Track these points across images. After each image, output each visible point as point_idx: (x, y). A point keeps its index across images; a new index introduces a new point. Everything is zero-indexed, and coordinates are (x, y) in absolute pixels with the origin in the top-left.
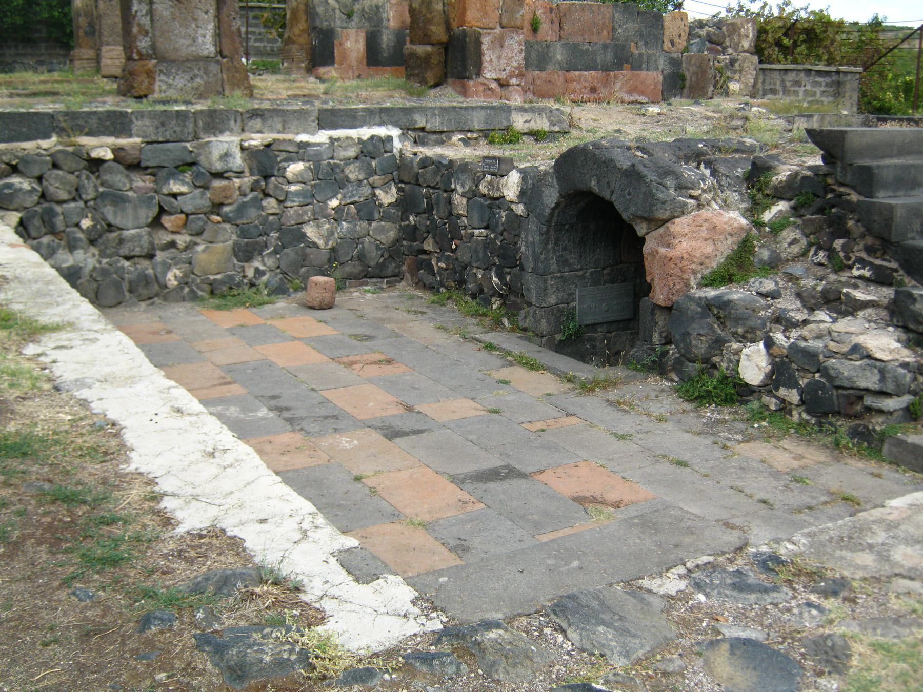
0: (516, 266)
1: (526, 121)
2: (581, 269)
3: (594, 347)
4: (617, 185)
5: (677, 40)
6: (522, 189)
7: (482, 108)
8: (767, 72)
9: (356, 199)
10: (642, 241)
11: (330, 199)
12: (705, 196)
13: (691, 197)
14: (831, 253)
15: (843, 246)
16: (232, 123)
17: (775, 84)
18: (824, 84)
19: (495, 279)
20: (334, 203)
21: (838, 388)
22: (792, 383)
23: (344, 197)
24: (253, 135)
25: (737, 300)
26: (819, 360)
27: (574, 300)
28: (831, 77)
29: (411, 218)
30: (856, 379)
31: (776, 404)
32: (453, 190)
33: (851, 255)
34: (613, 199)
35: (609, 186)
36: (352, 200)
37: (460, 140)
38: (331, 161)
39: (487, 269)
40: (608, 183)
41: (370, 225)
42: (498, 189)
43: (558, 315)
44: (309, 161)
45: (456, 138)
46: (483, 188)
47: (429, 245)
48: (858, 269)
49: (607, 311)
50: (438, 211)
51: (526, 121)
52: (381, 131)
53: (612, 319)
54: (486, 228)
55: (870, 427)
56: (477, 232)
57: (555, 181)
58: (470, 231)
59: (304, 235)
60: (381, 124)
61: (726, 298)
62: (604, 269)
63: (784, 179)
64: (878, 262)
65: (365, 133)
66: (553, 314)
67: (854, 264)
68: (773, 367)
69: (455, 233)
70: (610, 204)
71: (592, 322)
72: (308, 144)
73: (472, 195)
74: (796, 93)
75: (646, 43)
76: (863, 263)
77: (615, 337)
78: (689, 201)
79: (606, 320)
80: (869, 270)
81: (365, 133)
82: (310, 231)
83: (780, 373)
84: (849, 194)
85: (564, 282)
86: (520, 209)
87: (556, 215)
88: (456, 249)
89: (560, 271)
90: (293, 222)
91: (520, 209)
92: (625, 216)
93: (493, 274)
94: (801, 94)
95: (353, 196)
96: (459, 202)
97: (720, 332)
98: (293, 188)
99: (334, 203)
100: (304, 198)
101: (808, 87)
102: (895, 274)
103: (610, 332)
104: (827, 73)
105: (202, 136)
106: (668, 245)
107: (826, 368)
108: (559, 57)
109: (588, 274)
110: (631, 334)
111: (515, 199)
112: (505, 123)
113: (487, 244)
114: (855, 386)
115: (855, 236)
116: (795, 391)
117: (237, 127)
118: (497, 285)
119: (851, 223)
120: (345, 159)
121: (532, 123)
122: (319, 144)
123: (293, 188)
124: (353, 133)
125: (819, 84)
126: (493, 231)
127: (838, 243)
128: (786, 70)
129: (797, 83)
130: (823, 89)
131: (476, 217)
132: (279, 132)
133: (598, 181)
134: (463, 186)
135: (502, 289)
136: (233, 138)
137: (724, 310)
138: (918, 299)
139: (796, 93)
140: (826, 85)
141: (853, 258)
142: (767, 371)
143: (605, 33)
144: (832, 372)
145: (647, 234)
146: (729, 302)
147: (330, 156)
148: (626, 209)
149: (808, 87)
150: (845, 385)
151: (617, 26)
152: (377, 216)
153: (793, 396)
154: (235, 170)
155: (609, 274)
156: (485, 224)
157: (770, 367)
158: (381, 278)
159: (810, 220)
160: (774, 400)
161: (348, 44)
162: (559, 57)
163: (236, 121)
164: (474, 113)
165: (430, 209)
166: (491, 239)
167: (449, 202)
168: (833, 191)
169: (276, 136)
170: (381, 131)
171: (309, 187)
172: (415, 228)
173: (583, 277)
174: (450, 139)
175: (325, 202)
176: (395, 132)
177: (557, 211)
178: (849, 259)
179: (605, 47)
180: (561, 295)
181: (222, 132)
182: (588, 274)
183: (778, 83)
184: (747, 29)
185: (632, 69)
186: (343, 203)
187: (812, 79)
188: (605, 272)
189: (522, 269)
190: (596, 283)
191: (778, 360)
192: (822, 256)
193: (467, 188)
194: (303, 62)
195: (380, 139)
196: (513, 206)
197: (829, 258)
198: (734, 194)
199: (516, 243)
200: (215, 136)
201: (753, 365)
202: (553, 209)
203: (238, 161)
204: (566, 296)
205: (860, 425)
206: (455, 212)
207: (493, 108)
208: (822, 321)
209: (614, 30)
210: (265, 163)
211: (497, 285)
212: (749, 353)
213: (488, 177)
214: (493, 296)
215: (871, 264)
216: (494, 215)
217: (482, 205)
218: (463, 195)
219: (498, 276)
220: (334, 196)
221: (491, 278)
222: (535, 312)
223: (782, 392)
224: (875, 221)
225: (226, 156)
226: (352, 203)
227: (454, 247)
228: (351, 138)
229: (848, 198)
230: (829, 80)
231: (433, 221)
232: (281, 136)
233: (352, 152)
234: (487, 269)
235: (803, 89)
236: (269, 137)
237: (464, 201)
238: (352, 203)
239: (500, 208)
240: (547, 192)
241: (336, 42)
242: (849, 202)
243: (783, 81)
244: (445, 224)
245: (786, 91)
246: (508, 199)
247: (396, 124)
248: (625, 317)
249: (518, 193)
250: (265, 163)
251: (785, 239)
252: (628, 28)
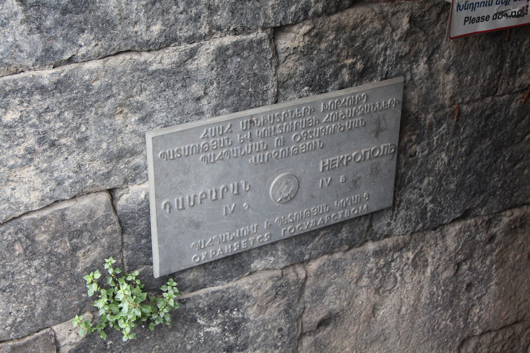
2: (168, 41)
27: (137, 174)
43: (63, 247)
49: (289, 200)
53: (309, 224)
62: (277, 31)
66: (31, 253)
71: (228, 249)
77: (320, 274)
79: (283, 233)
85: (80, 107)
89: (48, 57)
103: (303, 263)
109: (203, 61)
110: (377, 254)
155: (306, 52)
173: (179, 75)
180: (64, 166)
182: (203, 61)
188: (285, 42)
190: (241, 94)
204: (99, 166)
248: (364, 208)
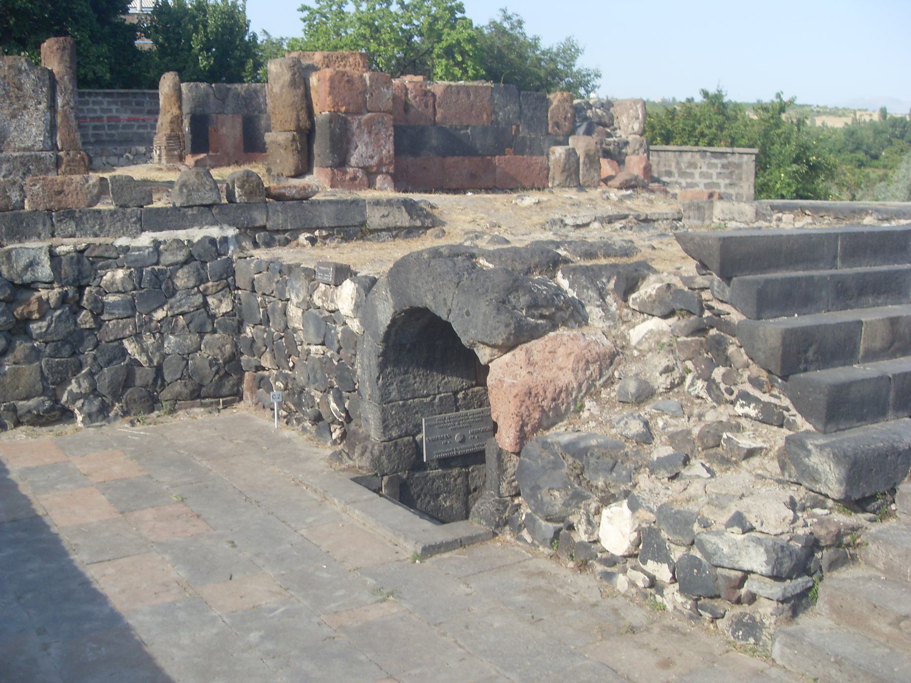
0: (354, 391)
1: (383, 216)
3: (447, 484)
4: (455, 302)
5: (562, 122)
6: (356, 301)
7: (330, 202)
8: (662, 154)
9: (185, 309)
10: (486, 369)
11: (155, 310)
12: (559, 314)
13: (542, 317)
14: (712, 386)
15: (724, 376)
16: (40, 227)
17: (670, 166)
18: (720, 166)
19: (333, 405)
20: (160, 314)
21: (717, 566)
22: (662, 556)
23: (171, 308)
24: (65, 240)
25: (597, 446)
26: (692, 531)
28: (726, 158)
29: (248, 330)
30: (737, 558)
31: (644, 580)
32: (288, 300)
33: (733, 388)
34: (451, 320)
35: (445, 304)
36: (180, 310)
37: (306, 239)
38: (156, 268)
39: (325, 391)
40: (445, 299)
41: (202, 338)
42: (332, 301)
44: (129, 268)
45: (303, 238)
47: (266, 362)
48: (742, 406)
50: (274, 322)
51: (383, 216)
52: (215, 232)
54: (323, 344)
55: (758, 619)
56: (313, 348)
57: (389, 295)
58: (306, 347)
59: (124, 352)
60: (214, 223)
61: (582, 445)
63: (654, 292)
64: (765, 398)
65: (197, 234)
66: (395, 450)
67: (737, 399)
68: (639, 534)
69: (292, 348)
70: (447, 326)
72: (127, 249)
73: (308, 305)
74: (691, 175)
75: (529, 127)
76: (746, 397)
78: (539, 321)
80: (754, 408)
81: (197, 234)
82: (130, 347)
83: (647, 545)
84: (728, 314)
86: (355, 325)
87: (393, 333)
88: (293, 367)
90: (112, 338)
91: (355, 325)
92: (464, 341)
93: (331, 398)
94: (697, 176)
95: (180, 306)
96: (295, 313)
97: (576, 486)
98: (111, 299)
99: (160, 314)
100: (124, 310)
101: (704, 169)
102: (785, 412)
104: (723, 154)
105: (5, 243)
107: (700, 541)
108: (434, 142)
111: (350, 313)
112: (359, 219)
113: (324, 362)
114: (737, 566)
115: (738, 365)
116: (666, 566)
117: (45, 231)
118: (335, 411)
119: (731, 349)
120: (172, 265)
121: (391, 218)
122: (139, 249)
123: (111, 299)
124: (181, 234)
125: (715, 165)
126: (330, 348)
127: (718, 373)
128: (681, 151)
129: (692, 165)
130: (719, 170)
131: (312, 330)
132: (96, 236)
133: (434, 297)
134: (297, 296)
135: (340, 417)
136: (40, 244)
137: (581, 459)
138: (814, 450)
139: (691, 175)
140: (723, 166)
141: (736, 393)
142: (632, 539)
143: (485, 116)
144: (708, 547)
145: (491, 361)
146: (586, 450)
147: (155, 261)
148: (466, 332)
149: (704, 169)
150: (725, 565)
151: (497, 109)
152: (209, 328)
153: (663, 573)
154: (44, 280)
156: (320, 341)
157: (635, 534)
158: (215, 397)
159: (685, 343)
160: (642, 575)
161: (224, 131)
162: (434, 142)
163: (44, 225)
164: (323, 209)
165: (266, 321)
168: (710, 308)
169: (91, 240)
170: (215, 232)
171: (130, 297)
172: (253, 341)
174: (296, 238)
175: (149, 313)
176: (231, 232)
177: (394, 329)
178: (731, 393)
179: (485, 130)
181: (28, 237)
183: (673, 164)
184: (637, 110)
185: (515, 153)
186: (169, 314)
187: (707, 161)
189: (359, 394)
191: (644, 525)
193: (301, 297)
194: (175, 150)
195: (212, 241)
196: (348, 321)
197: (709, 390)
198: (597, 309)
199: (353, 365)
200: (20, 242)
201: (616, 529)
202: (389, 327)
203: (45, 271)
205: (745, 614)
206: (291, 325)
207: (344, 202)
208: (699, 477)
209: (494, 112)
210: (79, 272)
211: (335, 411)
212: (610, 515)
214: (333, 422)
215: (757, 400)
216: (330, 330)
217: (316, 317)
218: (298, 306)
220: (161, 306)
221: (329, 404)
222: (373, 447)
223: (651, 566)
224: (759, 350)
225: (32, 264)
226: (183, 314)
227: (291, 364)
228: (178, 241)
229: (727, 317)
230: (725, 161)
231: (270, 334)
232: (97, 241)
233: (181, 257)
234: (325, 391)
235: (698, 170)
236: (82, 242)
237: (300, 312)
238: (183, 314)
239: (335, 322)
240: (380, 307)
241: (210, 128)
242: (728, 323)
243: (678, 163)
244: (281, 338)
245: (682, 174)
246: (343, 312)
247: (232, 224)
249: (352, 307)
250: (79, 272)
251: (656, 366)
252: (507, 111)
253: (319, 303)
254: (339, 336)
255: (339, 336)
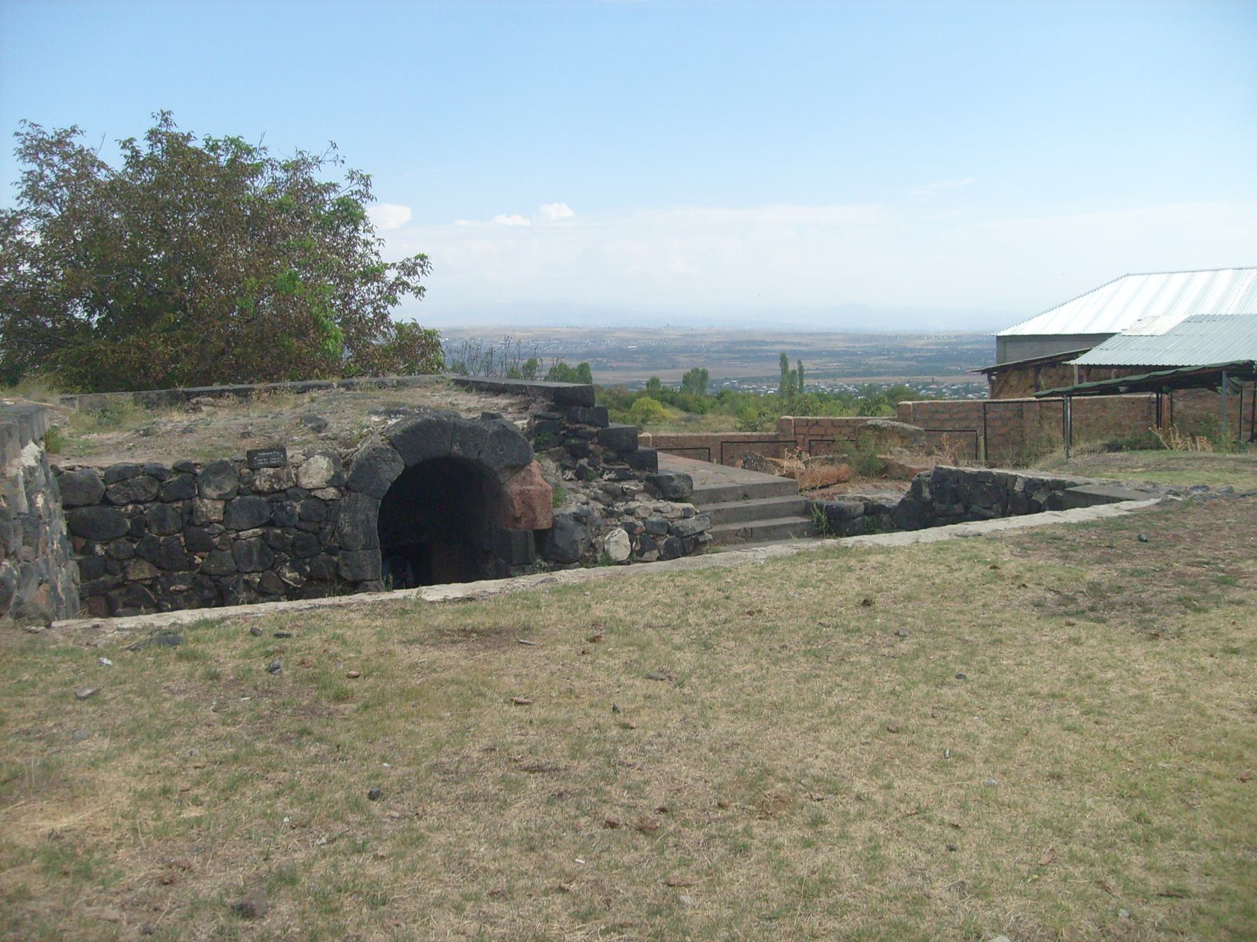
29: (98, 548)
34: (482, 456)
46: (261, 483)
58: (234, 535)
86: (331, 493)
106: (532, 484)
118: (294, 580)
127: (584, 461)
166: (277, 536)
167: (191, 511)
192: (569, 474)
193: (228, 487)
196: (319, 494)
213: (271, 471)
218: (220, 498)
219: (294, 568)
227: (198, 560)
237: (220, 505)
253: (267, 486)
254: (298, 510)
255: (298, 510)
